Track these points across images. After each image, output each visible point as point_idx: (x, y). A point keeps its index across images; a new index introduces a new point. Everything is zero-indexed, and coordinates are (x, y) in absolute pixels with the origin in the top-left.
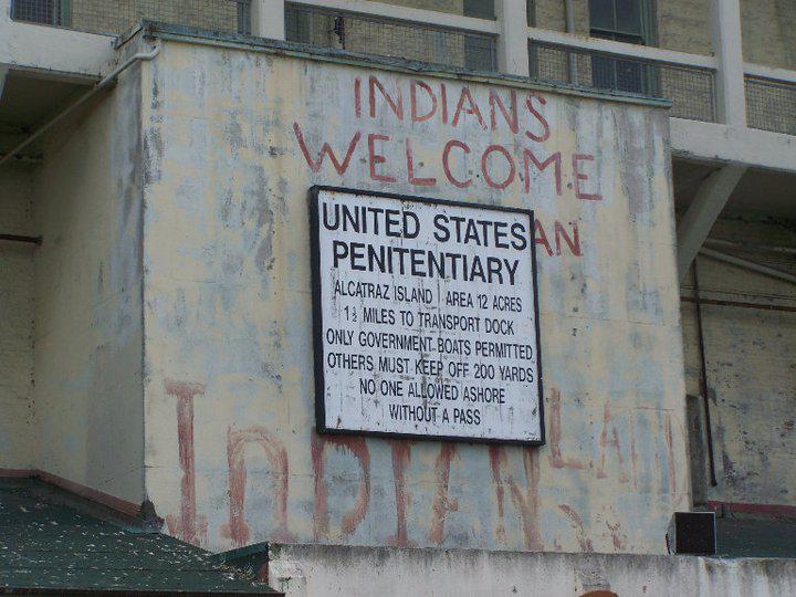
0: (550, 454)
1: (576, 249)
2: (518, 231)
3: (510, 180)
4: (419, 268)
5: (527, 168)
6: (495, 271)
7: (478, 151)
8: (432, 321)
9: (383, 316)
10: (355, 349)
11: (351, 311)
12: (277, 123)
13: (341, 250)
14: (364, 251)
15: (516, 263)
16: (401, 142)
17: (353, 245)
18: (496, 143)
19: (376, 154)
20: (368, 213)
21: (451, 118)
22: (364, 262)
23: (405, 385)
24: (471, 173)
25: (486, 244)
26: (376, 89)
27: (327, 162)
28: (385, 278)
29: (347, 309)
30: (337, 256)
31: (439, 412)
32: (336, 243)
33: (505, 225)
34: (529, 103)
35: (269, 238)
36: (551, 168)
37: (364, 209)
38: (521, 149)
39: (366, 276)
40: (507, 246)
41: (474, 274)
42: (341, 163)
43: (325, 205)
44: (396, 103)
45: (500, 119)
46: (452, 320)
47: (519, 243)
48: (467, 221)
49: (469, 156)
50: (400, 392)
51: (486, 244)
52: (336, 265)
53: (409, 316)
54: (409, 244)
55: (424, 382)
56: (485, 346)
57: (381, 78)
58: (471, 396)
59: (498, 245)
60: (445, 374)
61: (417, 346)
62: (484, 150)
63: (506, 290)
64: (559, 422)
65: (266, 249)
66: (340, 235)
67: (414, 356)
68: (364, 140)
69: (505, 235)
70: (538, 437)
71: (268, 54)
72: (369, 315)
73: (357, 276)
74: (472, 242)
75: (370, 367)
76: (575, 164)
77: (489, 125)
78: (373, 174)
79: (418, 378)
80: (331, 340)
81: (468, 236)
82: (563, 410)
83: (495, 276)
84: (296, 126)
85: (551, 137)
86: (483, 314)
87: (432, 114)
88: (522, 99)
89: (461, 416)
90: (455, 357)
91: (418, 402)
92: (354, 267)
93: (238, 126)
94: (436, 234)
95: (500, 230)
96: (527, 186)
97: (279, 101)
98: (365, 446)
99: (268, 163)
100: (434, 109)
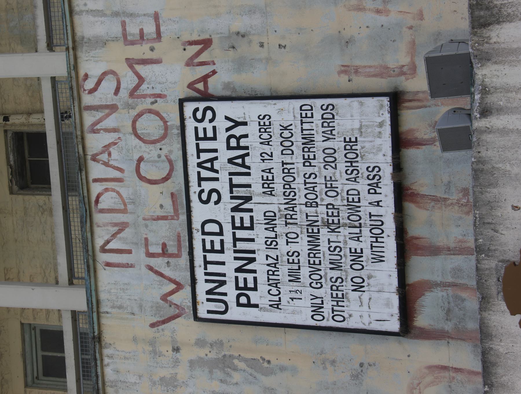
0: (403, 78)
1: (206, 43)
2: (199, 115)
3: (157, 114)
4: (247, 223)
5: (144, 96)
6: (238, 143)
7: (140, 147)
8: (291, 213)
9: (293, 262)
10: (325, 292)
11: (294, 295)
12: (152, 343)
13: (243, 300)
14: (241, 276)
15: (227, 118)
16: (146, 226)
17: (237, 288)
18: (130, 130)
19: (160, 251)
20: (209, 271)
21: (117, 174)
22: (250, 277)
23: (353, 245)
24: (159, 156)
25: (215, 151)
26: (107, 248)
27: (176, 298)
28: (260, 257)
29: (292, 299)
30: (249, 305)
31: (374, 210)
32: (239, 305)
33: (196, 129)
34: (91, 91)
35: (246, 360)
36: (141, 69)
37: (206, 274)
38: (131, 101)
39: (262, 278)
40: (214, 128)
41: (243, 165)
42: (173, 286)
43: (209, 312)
44: (116, 229)
45: (110, 122)
46: (288, 191)
47: (209, 114)
48: (200, 169)
49: (146, 156)
50: (359, 251)
51: (215, 151)
52: (256, 306)
53: (288, 235)
54: (228, 229)
55: (345, 225)
56: (306, 157)
57: (99, 242)
58: (353, 175)
59: (214, 138)
60: (338, 202)
61: (316, 231)
62: (137, 141)
63: (252, 129)
64: (370, 67)
65: (252, 363)
66: (231, 299)
67: (324, 234)
68: (154, 262)
69: (205, 129)
70: (386, 101)
71: (101, 347)
72: (294, 277)
73: (263, 287)
74: (217, 165)
75: (339, 280)
76: (133, 43)
77: (115, 135)
78: (178, 256)
79: (345, 232)
80: (320, 318)
81: (212, 169)
82: (357, 62)
83: (243, 142)
84: (153, 325)
85: (118, 72)
86: (278, 158)
87: (118, 193)
88: (87, 100)
89: (374, 188)
90: (320, 188)
91: (366, 231)
92: (255, 289)
93: (162, 379)
94: (217, 203)
95: (201, 135)
96: (160, 96)
97: (135, 339)
98: (411, 285)
99: (186, 355)
100: (113, 190)
